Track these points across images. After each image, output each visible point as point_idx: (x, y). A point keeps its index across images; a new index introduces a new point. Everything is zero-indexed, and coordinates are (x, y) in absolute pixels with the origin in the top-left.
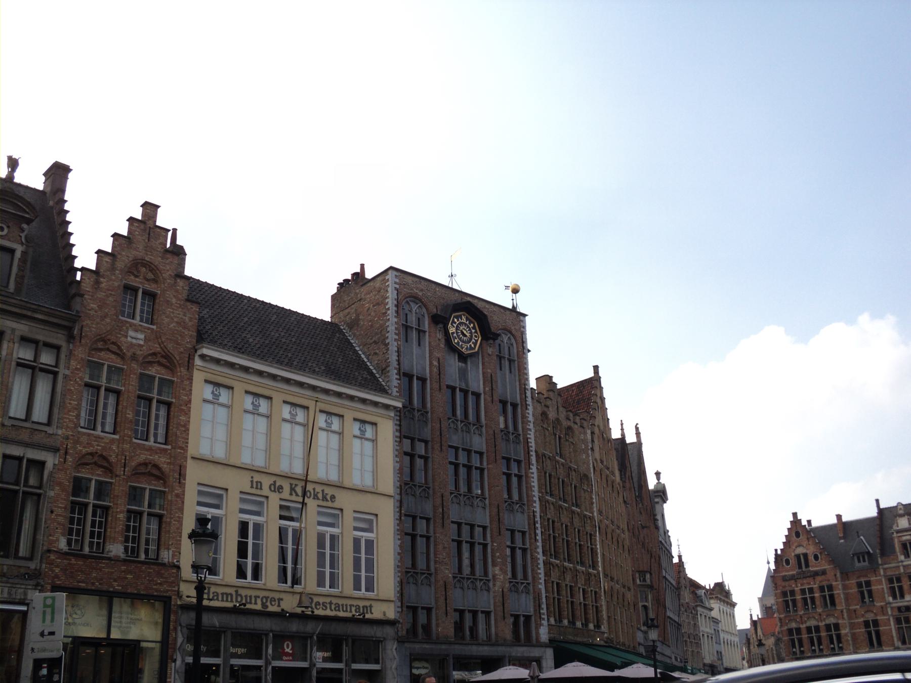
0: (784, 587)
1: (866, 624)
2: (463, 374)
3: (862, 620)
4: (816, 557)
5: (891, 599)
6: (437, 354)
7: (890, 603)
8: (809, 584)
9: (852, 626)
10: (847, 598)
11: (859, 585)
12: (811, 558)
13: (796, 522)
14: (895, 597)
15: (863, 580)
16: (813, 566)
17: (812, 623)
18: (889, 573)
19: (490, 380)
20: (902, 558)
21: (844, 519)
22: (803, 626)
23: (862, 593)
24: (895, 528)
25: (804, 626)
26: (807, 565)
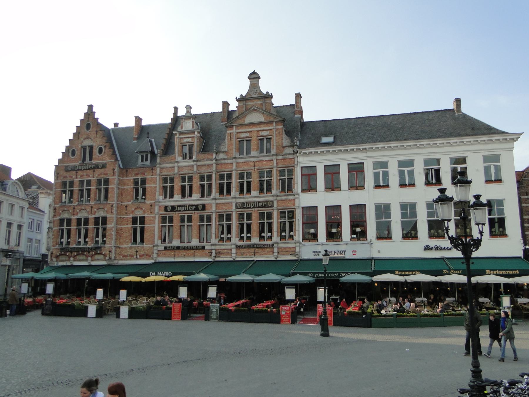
0: (64, 177)
3: (131, 216)
4: (100, 151)
5: (161, 198)
7: (159, 202)
8: (88, 176)
9: (119, 221)
10: (121, 194)
11: (136, 182)
12: (96, 151)
13: (90, 114)
14: (165, 197)
15: (140, 177)
16: (95, 159)
17: (83, 215)
18: (165, 173)
20: (180, 159)
21: (144, 123)
22: (74, 218)
23: (137, 190)
24: (179, 129)
25: (76, 217)
26: (91, 159)
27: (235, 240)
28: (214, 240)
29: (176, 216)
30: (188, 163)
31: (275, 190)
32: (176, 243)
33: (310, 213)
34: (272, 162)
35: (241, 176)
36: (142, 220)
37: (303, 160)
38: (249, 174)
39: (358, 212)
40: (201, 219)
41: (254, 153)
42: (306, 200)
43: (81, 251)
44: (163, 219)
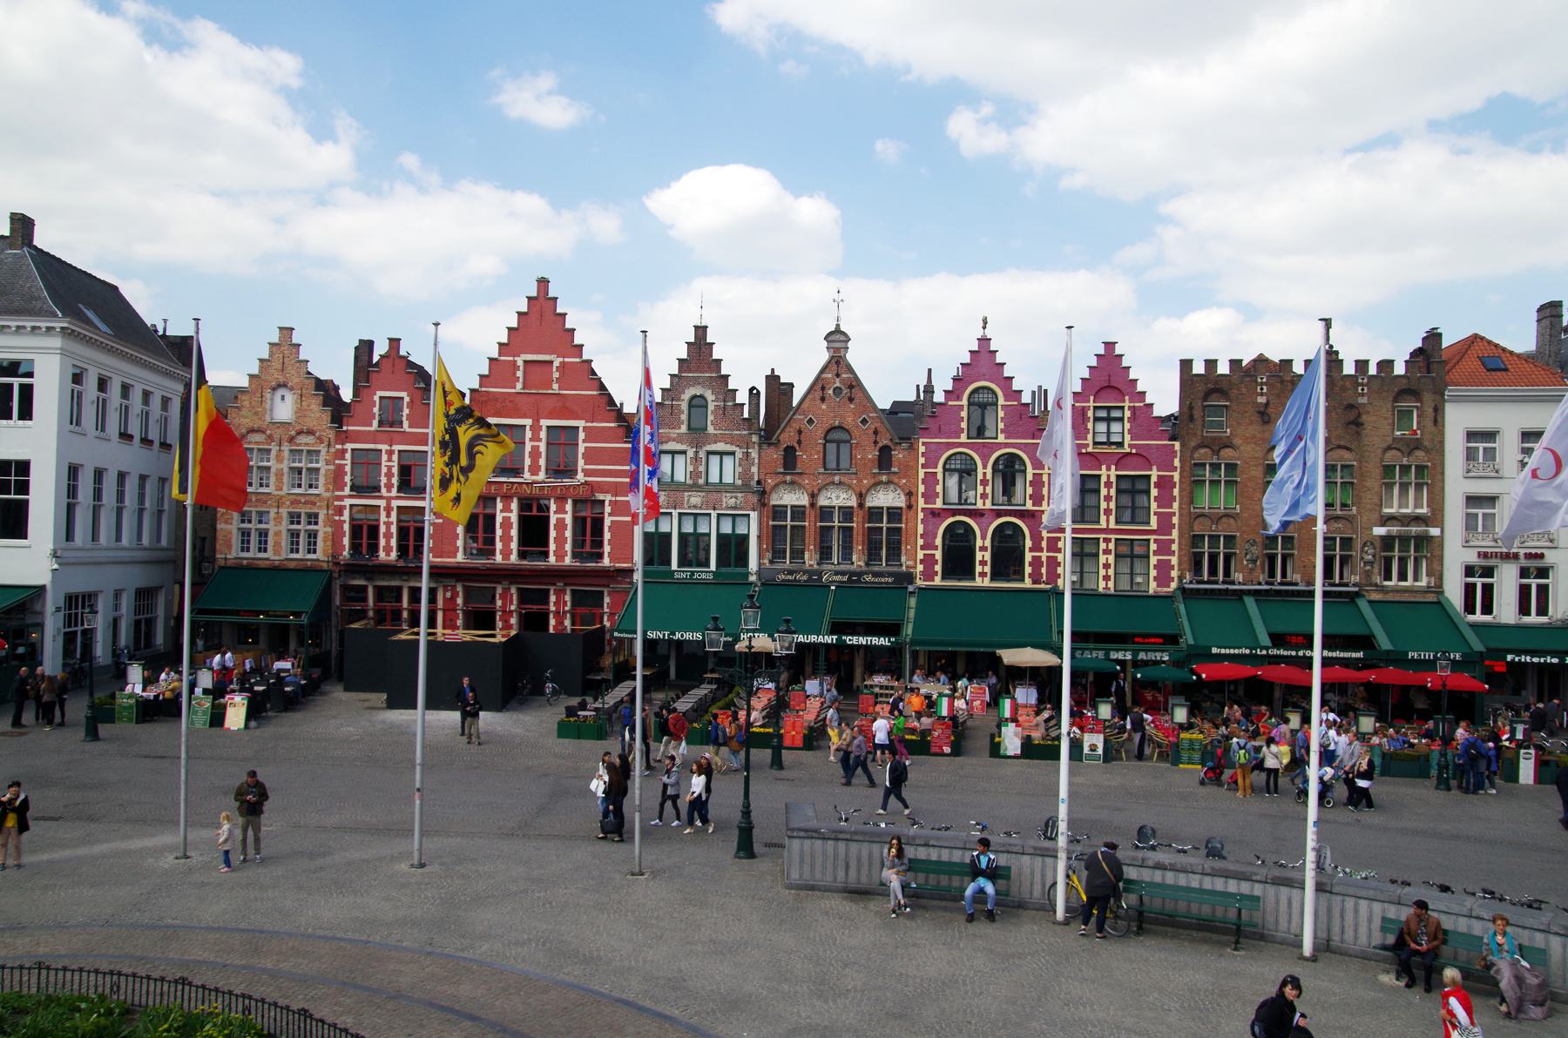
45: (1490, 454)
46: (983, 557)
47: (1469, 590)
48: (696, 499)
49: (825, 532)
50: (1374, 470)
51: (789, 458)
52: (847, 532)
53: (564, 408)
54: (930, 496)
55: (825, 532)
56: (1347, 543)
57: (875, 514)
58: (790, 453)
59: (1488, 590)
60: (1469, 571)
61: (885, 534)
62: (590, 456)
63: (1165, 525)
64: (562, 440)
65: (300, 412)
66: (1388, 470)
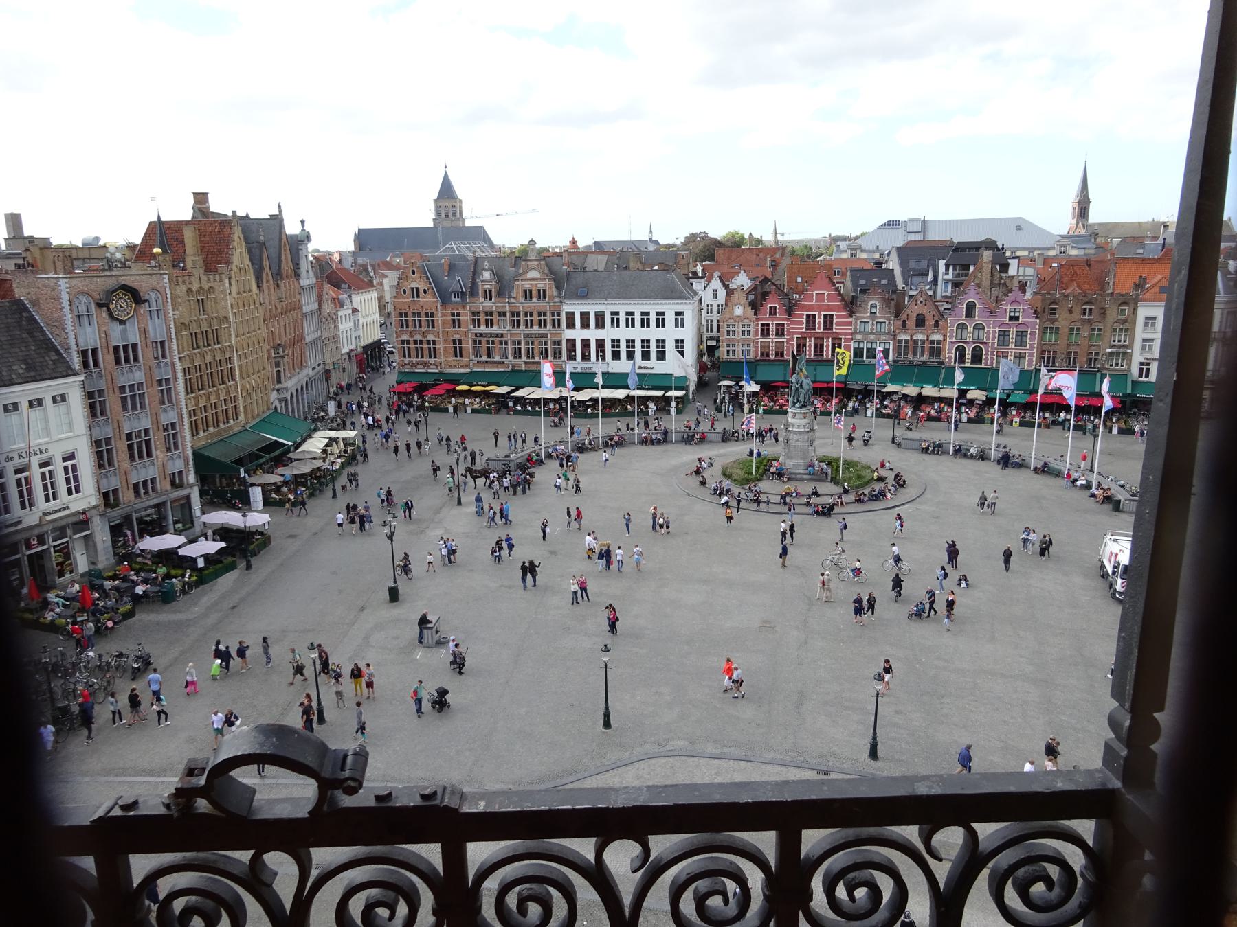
1: (454, 342)
2: (124, 332)
6: (103, 329)
9: (445, 342)
12: (421, 291)
17: (418, 337)
19: (144, 333)
27: (524, 358)
28: (510, 358)
29: (484, 340)
30: (488, 303)
31: (549, 327)
32: (485, 358)
33: (571, 343)
34: (545, 306)
35: (526, 315)
36: (460, 342)
37: (567, 308)
38: (531, 315)
39: (601, 344)
40: (501, 343)
41: (535, 300)
42: (569, 334)
43: (418, 363)
44: (475, 342)
45: (1154, 324)
46: (968, 356)
47: (1141, 370)
48: (872, 337)
49: (915, 349)
50: (1109, 330)
51: (904, 324)
52: (923, 348)
53: (829, 308)
54: (951, 337)
55: (915, 349)
56: (1097, 354)
57: (932, 342)
58: (904, 322)
59: (1148, 370)
60: (1142, 364)
61: (935, 349)
62: (837, 324)
63: (1032, 347)
64: (828, 321)
65: (744, 313)
66: (1115, 330)
